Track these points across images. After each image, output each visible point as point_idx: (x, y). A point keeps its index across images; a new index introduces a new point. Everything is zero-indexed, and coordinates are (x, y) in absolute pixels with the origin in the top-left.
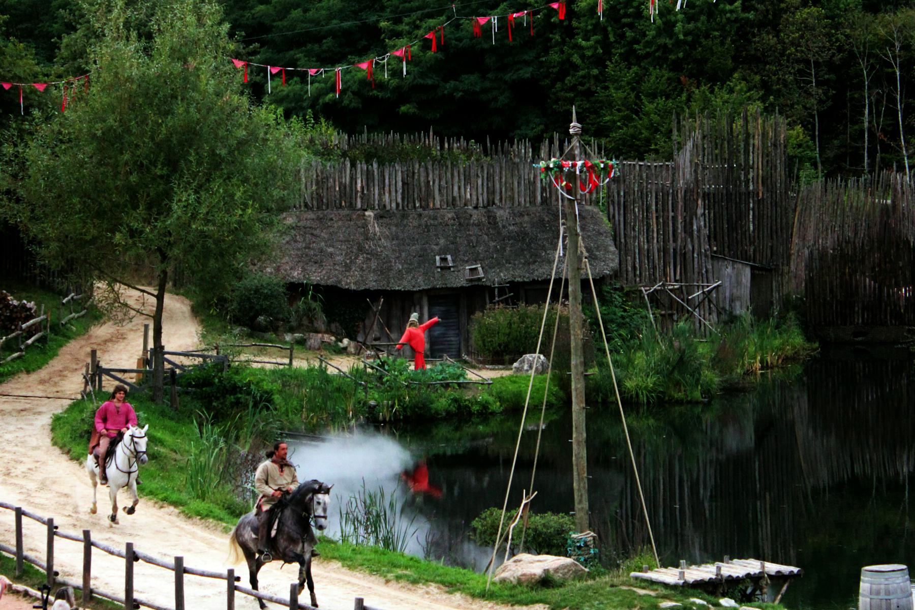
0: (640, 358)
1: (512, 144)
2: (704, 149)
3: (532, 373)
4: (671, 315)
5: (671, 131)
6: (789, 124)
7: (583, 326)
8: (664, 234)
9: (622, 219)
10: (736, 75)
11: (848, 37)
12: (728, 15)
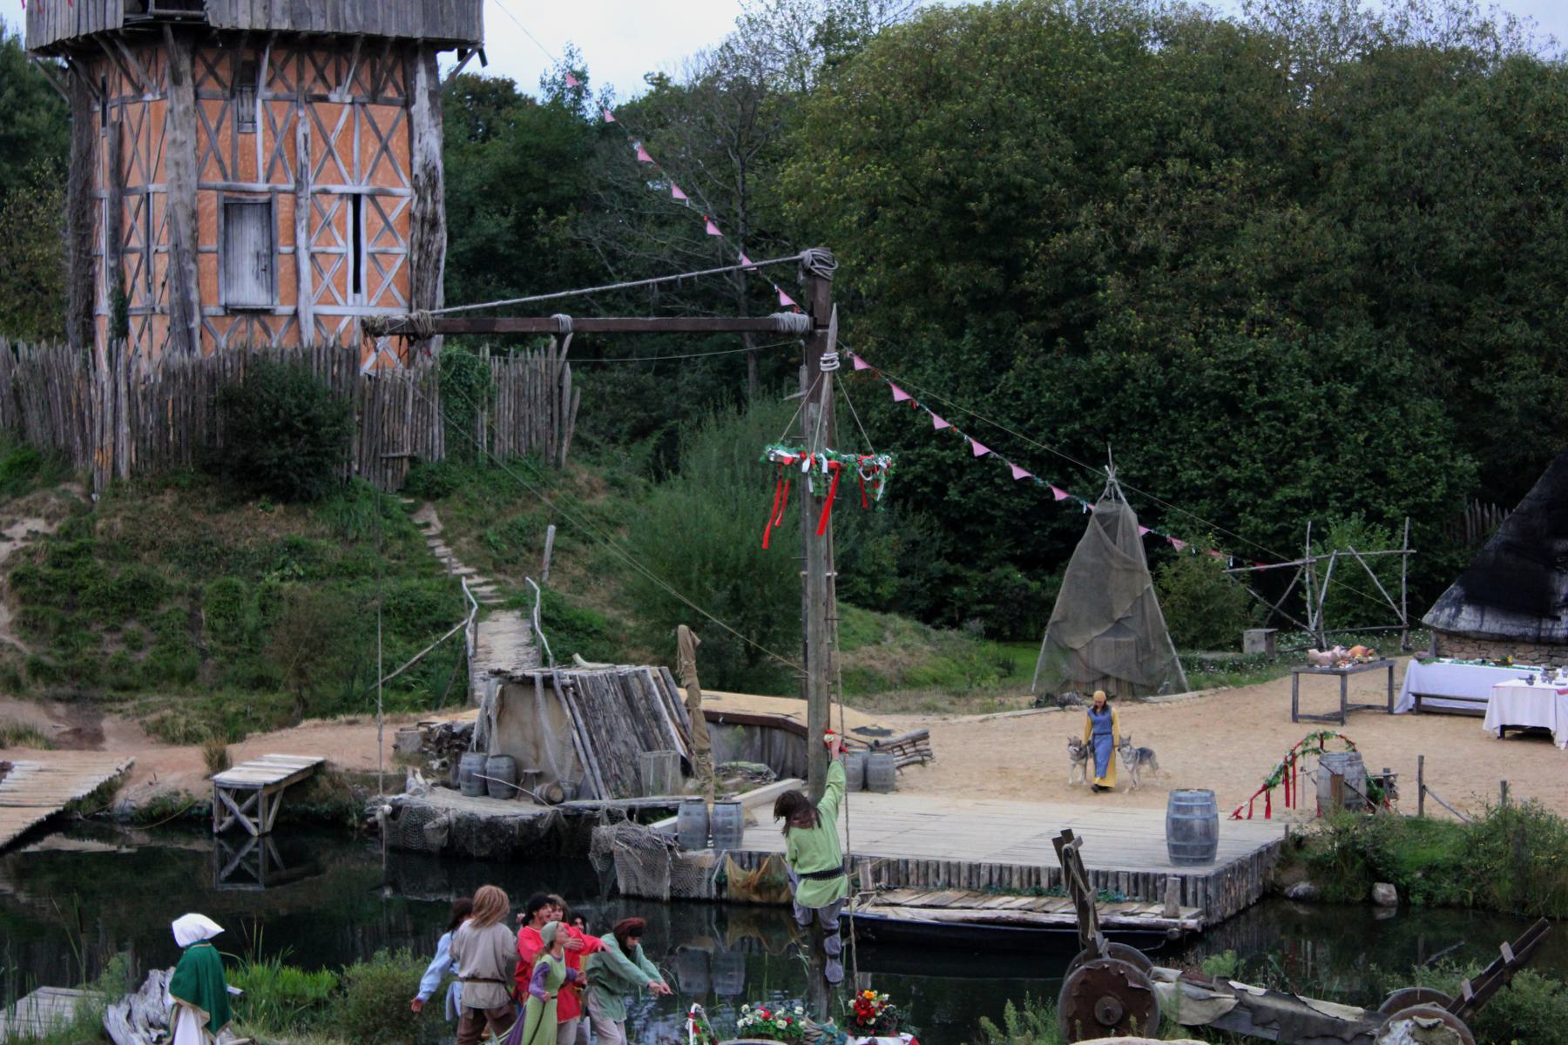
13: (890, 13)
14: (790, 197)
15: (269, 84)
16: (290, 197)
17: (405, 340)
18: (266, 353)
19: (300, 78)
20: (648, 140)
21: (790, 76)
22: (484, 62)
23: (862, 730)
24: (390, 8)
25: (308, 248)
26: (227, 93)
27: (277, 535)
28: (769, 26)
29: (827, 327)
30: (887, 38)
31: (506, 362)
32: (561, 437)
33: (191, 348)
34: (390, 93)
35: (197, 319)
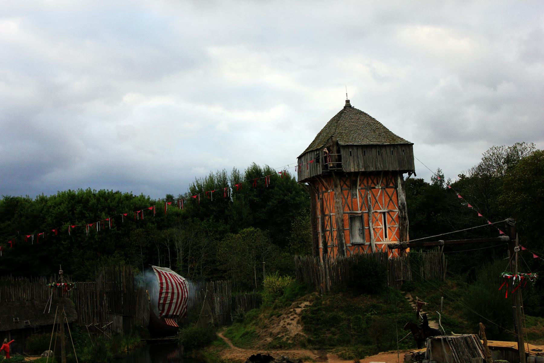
0: (86, 350)
1: (39, 278)
2: (106, 277)
3: (48, 357)
4: (96, 334)
5: (94, 271)
6: (134, 268)
7: (65, 340)
8: (93, 307)
9: (78, 302)
10: (116, 252)
11: (152, 238)
12: (112, 232)
13: (524, 153)
14: (500, 204)
15: (360, 185)
16: (367, 214)
17: (400, 250)
18: (363, 255)
19: (368, 183)
20: (461, 192)
21: (498, 173)
22: (415, 175)
23: (533, 350)
24: (390, 163)
25: (372, 227)
26: (349, 188)
27: (369, 303)
28: (491, 160)
29: (515, 239)
30: (524, 160)
31: (427, 254)
32: (443, 273)
33: (344, 255)
34: (391, 185)
35: (345, 247)
